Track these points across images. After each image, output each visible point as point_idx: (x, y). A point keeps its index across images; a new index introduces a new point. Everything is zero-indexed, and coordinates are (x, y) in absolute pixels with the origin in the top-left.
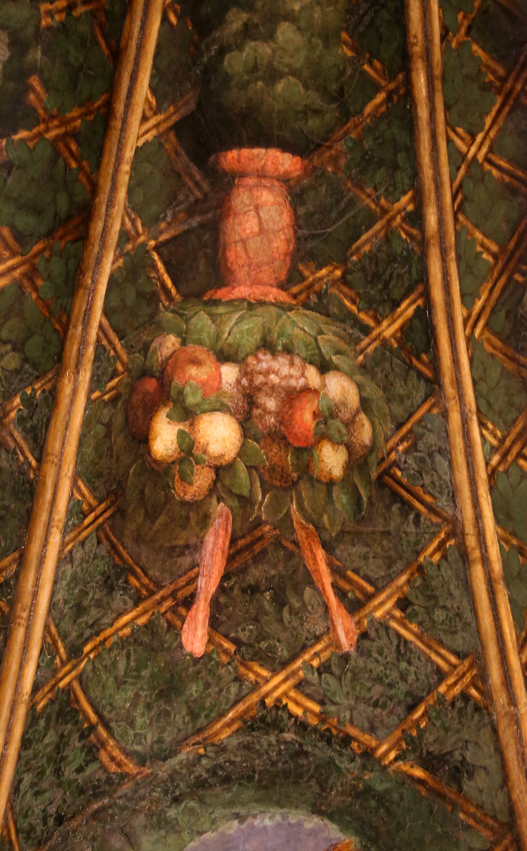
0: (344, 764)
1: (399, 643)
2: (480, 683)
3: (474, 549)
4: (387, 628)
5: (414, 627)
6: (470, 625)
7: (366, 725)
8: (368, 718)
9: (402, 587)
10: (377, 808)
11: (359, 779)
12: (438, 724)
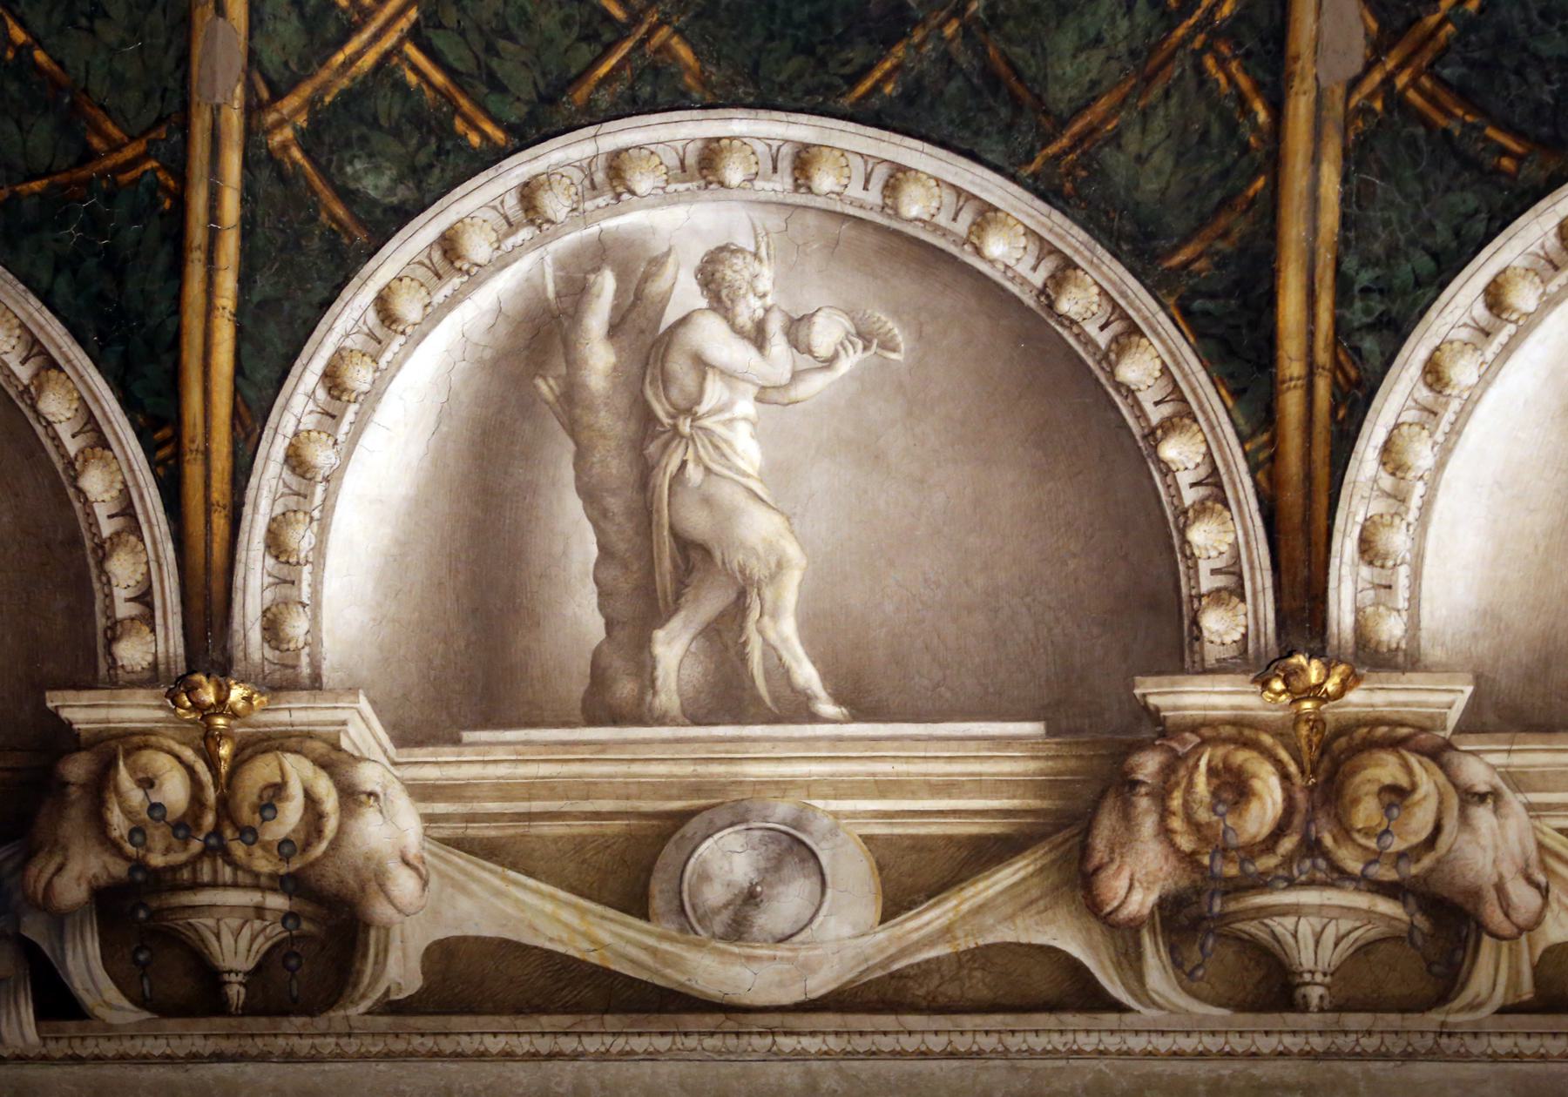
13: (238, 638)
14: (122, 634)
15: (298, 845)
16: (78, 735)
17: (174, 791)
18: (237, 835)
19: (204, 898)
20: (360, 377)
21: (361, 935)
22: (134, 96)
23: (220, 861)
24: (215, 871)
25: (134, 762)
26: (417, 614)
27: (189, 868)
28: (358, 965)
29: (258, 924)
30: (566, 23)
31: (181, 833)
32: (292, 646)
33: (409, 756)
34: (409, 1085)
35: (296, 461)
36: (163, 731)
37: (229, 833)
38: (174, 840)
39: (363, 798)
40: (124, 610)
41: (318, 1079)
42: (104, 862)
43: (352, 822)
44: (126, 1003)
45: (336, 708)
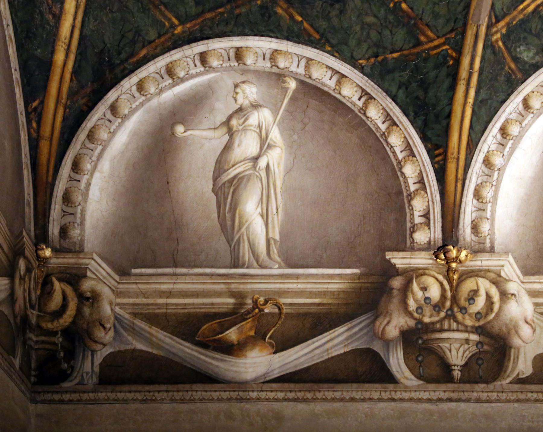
13: (461, 232)
14: (417, 230)
15: (483, 314)
16: (398, 269)
17: (435, 293)
18: (459, 310)
19: (445, 335)
20: (514, 130)
21: (508, 351)
22: (442, 21)
23: (452, 321)
24: (450, 324)
25: (419, 280)
26: (533, 223)
27: (440, 323)
28: (506, 364)
29: (466, 346)
31: (437, 309)
32: (483, 235)
33: (529, 279)
34: (527, 413)
35: (487, 162)
36: (431, 268)
37: (456, 309)
38: (434, 312)
39: (510, 296)
40: (418, 220)
41: (490, 410)
42: (406, 320)
43: (505, 306)
44: (413, 377)
45: (500, 260)
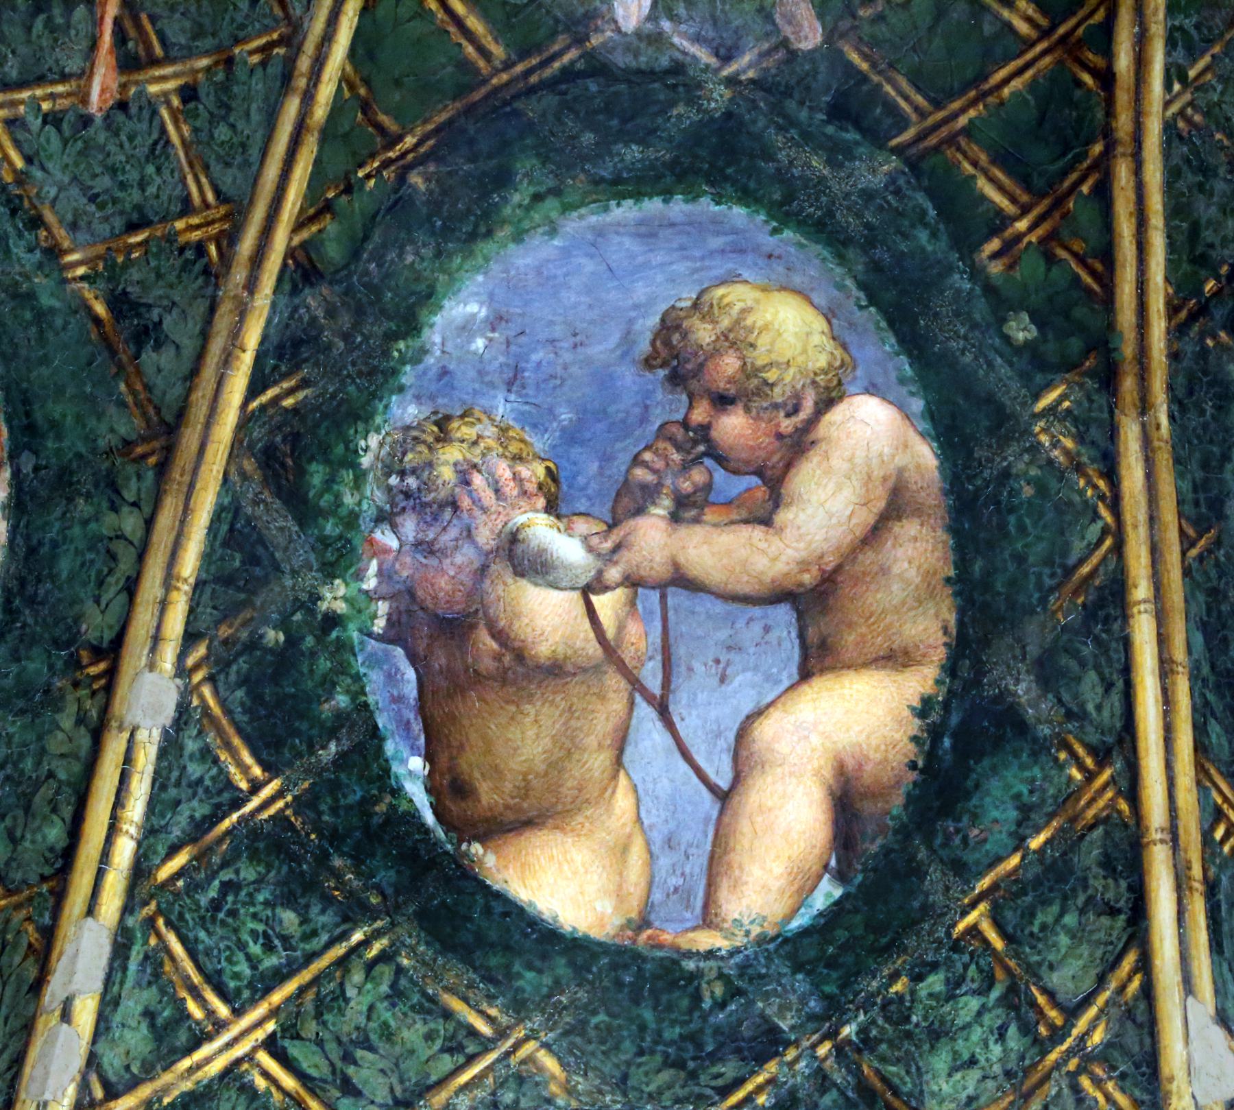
0: (18, 250)
1: (160, 139)
2: (225, 243)
3: (302, 75)
4: (155, 113)
5: (186, 130)
6: (250, 165)
7: (69, 217)
8: (76, 210)
9: (197, 71)
10: (30, 324)
11: (27, 277)
12: (153, 263)
30: (429, 1037)
